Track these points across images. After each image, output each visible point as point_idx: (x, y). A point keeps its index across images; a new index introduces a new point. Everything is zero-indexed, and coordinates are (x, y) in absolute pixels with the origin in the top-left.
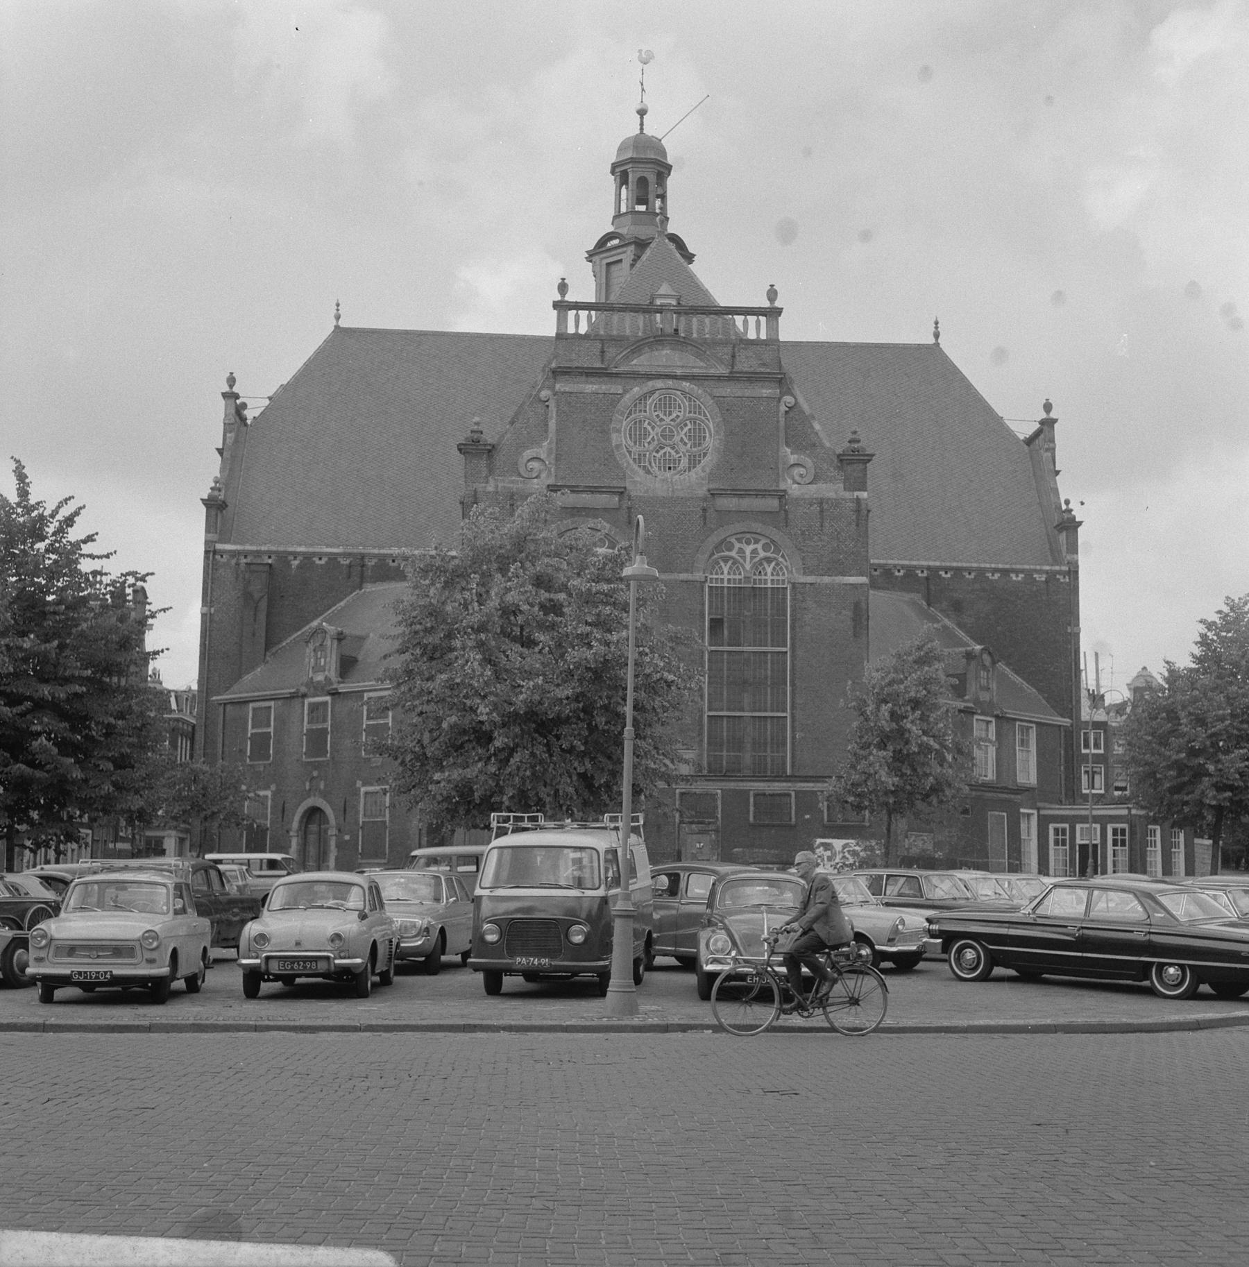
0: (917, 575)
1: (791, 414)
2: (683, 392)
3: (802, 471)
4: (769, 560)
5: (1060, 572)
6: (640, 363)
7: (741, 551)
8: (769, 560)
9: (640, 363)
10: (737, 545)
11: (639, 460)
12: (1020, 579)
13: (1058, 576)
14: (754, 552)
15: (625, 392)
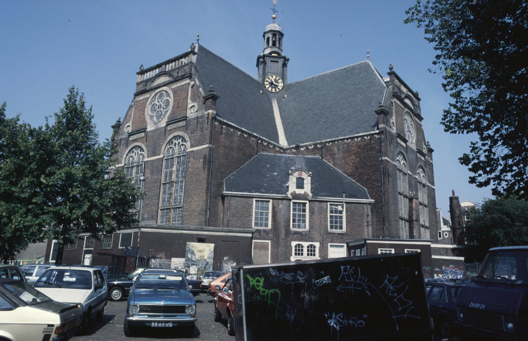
0: (318, 147)
1: (194, 87)
2: (165, 91)
3: (194, 108)
4: (183, 145)
5: (375, 134)
6: (155, 84)
7: (175, 143)
8: (183, 145)
9: (155, 84)
10: (174, 141)
11: (151, 117)
12: (359, 140)
13: (375, 136)
14: (179, 143)
15: (150, 96)
